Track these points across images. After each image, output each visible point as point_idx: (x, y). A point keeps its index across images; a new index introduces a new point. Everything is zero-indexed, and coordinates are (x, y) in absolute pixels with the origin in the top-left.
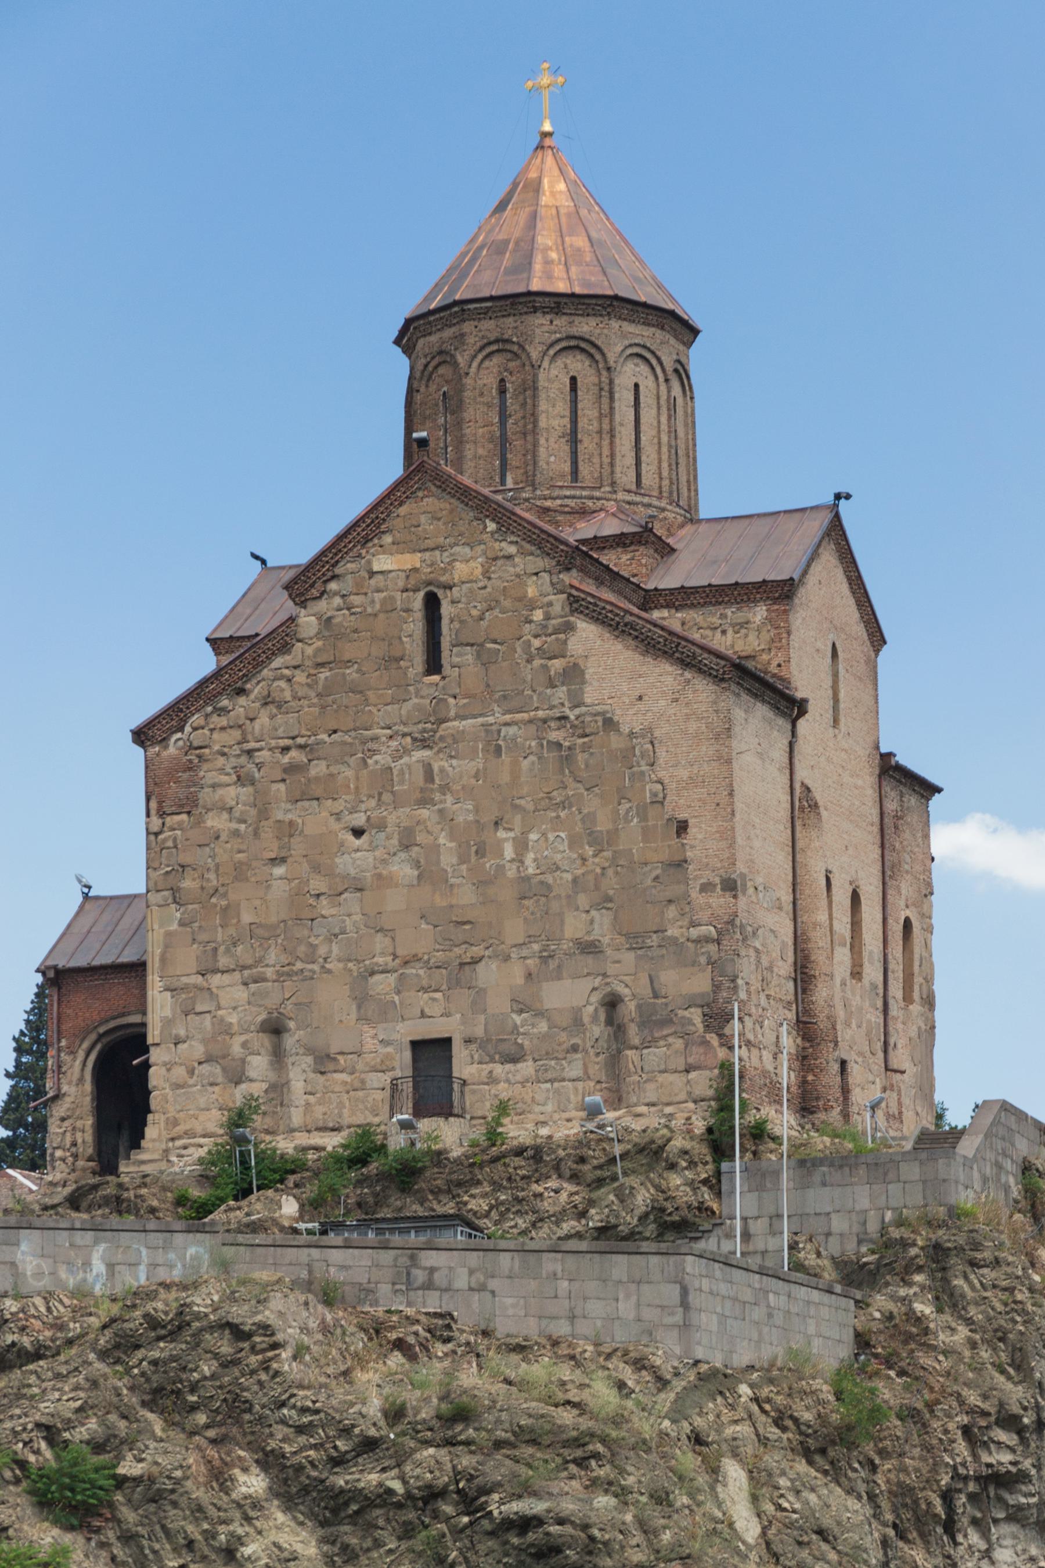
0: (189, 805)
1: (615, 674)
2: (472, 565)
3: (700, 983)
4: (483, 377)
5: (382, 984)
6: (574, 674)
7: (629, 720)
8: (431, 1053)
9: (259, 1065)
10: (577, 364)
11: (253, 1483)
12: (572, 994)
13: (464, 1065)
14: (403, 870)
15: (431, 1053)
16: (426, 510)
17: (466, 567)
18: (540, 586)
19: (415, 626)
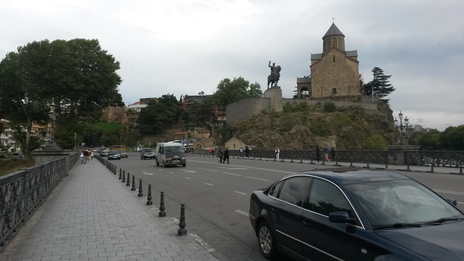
0: (314, 71)
1: (349, 62)
2: (337, 54)
3: (356, 85)
4: (332, 40)
5: (330, 84)
6: (346, 62)
7: (350, 66)
8: (334, 90)
9: (321, 90)
10: (339, 40)
11: (364, 119)
12: (346, 85)
13: (337, 90)
14: (332, 76)
15: (334, 90)
16: (334, 50)
17: (337, 55)
18: (343, 56)
19: (333, 59)
